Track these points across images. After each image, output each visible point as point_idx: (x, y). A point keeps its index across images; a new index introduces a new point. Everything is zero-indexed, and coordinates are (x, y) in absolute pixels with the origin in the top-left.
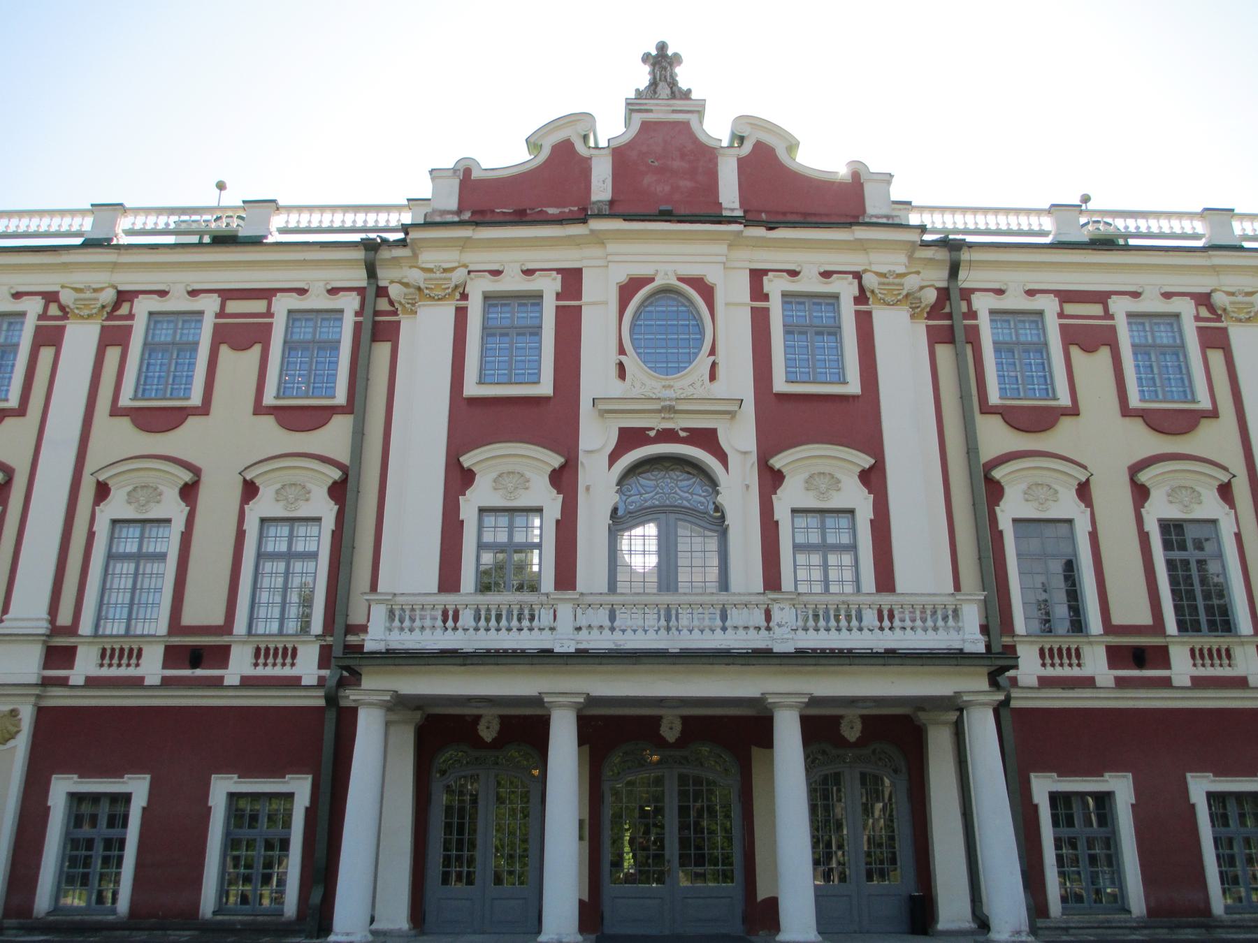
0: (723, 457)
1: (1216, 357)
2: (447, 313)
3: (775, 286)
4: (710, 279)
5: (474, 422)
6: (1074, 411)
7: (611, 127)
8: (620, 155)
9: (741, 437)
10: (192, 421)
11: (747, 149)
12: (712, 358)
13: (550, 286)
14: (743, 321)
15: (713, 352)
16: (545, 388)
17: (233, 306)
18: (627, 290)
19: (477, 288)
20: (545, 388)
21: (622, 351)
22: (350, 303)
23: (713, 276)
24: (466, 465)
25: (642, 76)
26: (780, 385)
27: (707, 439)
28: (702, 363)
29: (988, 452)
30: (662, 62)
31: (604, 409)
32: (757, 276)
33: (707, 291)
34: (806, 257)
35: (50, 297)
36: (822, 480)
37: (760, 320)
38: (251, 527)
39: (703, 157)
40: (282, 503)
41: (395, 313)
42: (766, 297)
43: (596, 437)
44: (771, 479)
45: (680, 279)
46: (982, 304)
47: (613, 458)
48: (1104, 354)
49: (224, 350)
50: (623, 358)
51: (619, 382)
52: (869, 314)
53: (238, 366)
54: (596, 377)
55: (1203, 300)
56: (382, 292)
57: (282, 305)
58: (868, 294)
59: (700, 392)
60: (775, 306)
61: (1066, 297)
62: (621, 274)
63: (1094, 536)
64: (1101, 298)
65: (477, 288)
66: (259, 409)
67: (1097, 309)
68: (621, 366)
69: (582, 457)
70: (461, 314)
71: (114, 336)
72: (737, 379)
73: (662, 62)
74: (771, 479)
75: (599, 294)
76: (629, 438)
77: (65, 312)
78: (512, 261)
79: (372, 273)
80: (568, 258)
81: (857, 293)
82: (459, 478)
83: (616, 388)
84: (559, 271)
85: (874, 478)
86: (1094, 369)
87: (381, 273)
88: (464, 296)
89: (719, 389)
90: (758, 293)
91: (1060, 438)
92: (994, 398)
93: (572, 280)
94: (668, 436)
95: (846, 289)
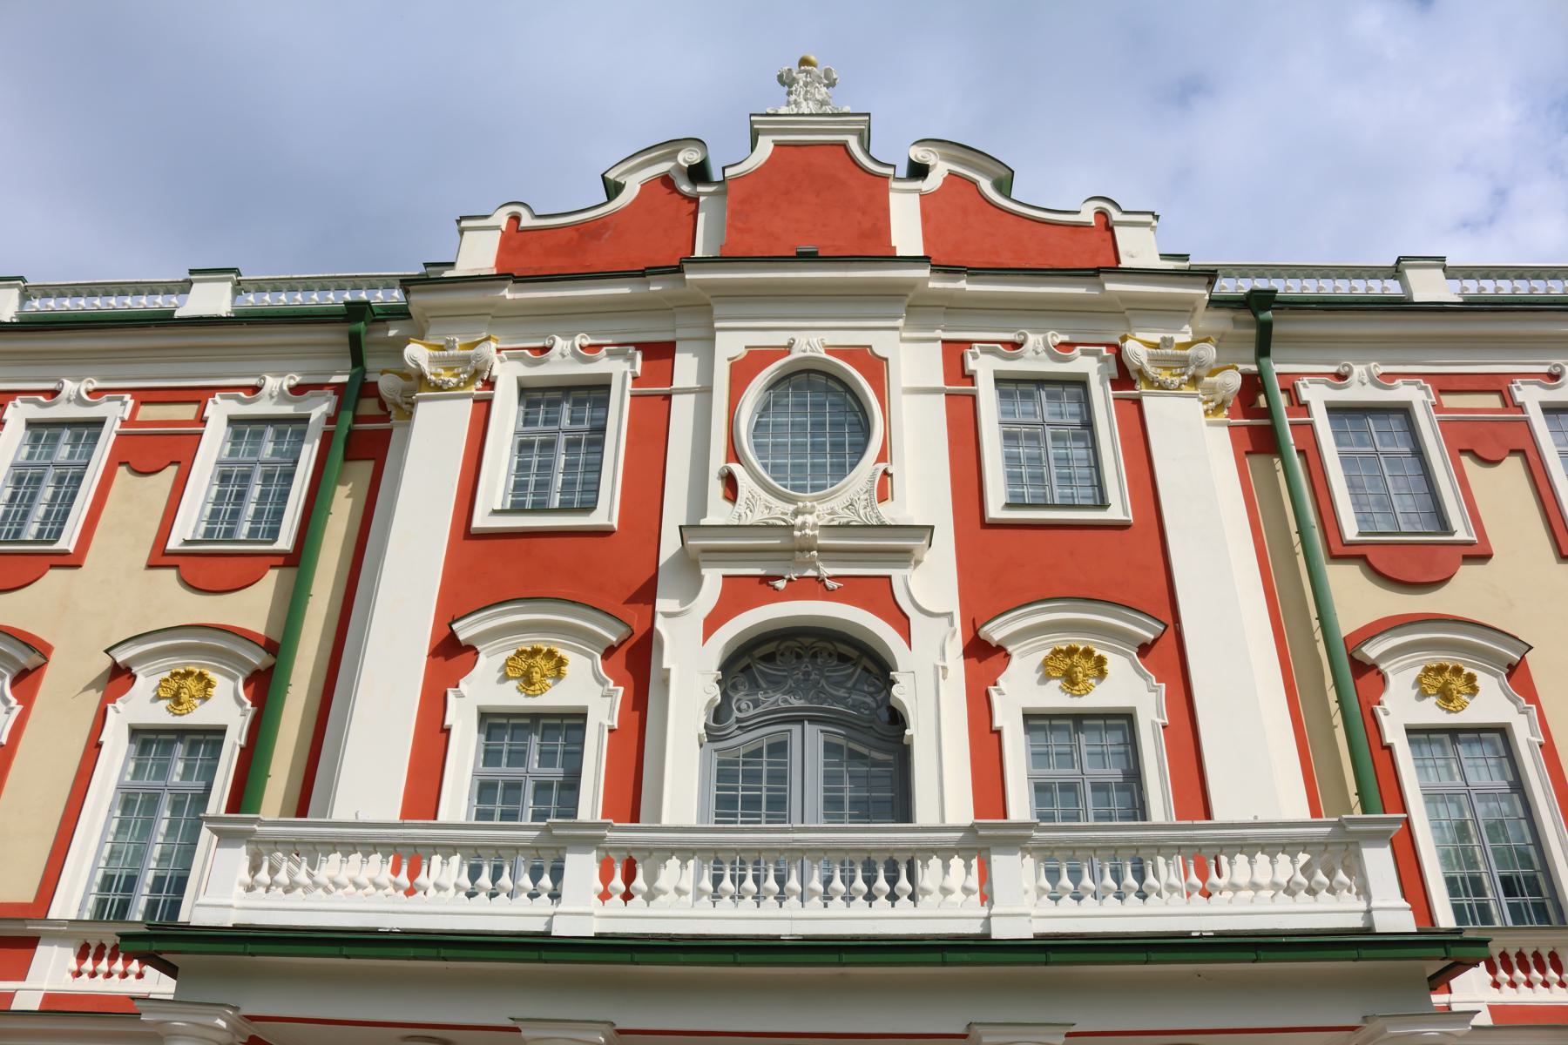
0: (902, 624)
2: (460, 412)
3: (984, 367)
4: (879, 351)
5: (488, 566)
6: (1479, 554)
9: (932, 582)
10: (54, 579)
11: (934, 181)
12: (882, 466)
15: (882, 457)
17: (149, 413)
19: (507, 375)
20: (606, 513)
21: (734, 454)
23: (882, 341)
24: (462, 636)
29: (1347, 622)
32: (955, 353)
33: (875, 367)
38: (116, 742)
40: (164, 703)
41: (386, 418)
42: (971, 378)
44: (983, 654)
45: (828, 352)
46: (1316, 395)
47: (712, 624)
48: (1513, 464)
49: (122, 471)
50: (736, 468)
51: (729, 505)
52: (1138, 402)
53: (139, 497)
56: (368, 389)
57: (219, 411)
58: (1134, 376)
59: (863, 515)
61: (1445, 385)
62: (731, 344)
63: (1549, 750)
64: (1498, 385)
65: (507, 375)
66: (161, 558)
67: (1493, 401)
68: (730, 482)
69: (661, 624)
70: (484, 406)
72: (921, 490)
79: (357, 359)
81: (1114, 372)
82: (450, 654)
83: (719, 512)
84: (638, 346)
85: (1167, 655)
86: (1502, 490)
87: (371, 364)
88: (490, 384)
89: (890, 513)
90: (957, 371)
91: (1464, 593)
92: (1351, 531)
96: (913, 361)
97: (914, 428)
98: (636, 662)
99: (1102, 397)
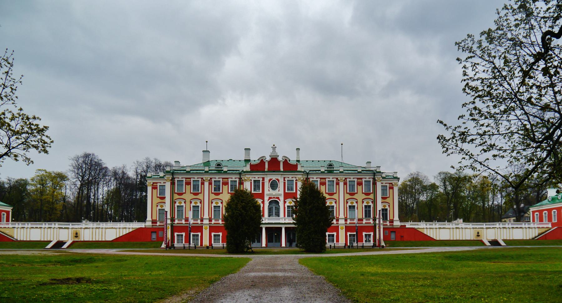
1: (338, 186)
3: (286, 179)
7: (268, 159)
8: (269, 162)
9: (282, 198)
13: (261, 179)
14: (283, 183)
16: (261, 192)
18: (270, 180)
20: (261, 192)
22: (238, 180)
23: (279, 179)
25: (271, 150)
26: (286, 191)
27: (278, 198)
28: (278, 189)
30: (274, 148)
31: (268, 195)
32: (284, 178)
33: (278, 180)
34: (290, 176)
35: (202, 178)
36: (290, 203)
37: (285, 183)
39: (279, 162)
43: (266, 198)
44: (285, 202)
54: (266, 192)
55: (337, 179)
60: (286, 182)
62: (269, 179)
71: (210, 184)
72: (282, 192)
73: (274, 148)
74: (285, 202)
75: (266, 180)
76: (270, 198)
77: (204, 181)
78: (257, 177)
80: (263, 176)
83: (268, 193)
89: (280, 193)
90: (284, 180)
93: (263, 179)
94: (274, 198)
95: (294, 179)
96: (281, 180)
97: (281, 185)
98: (263, 202)
99: (295, 182)
